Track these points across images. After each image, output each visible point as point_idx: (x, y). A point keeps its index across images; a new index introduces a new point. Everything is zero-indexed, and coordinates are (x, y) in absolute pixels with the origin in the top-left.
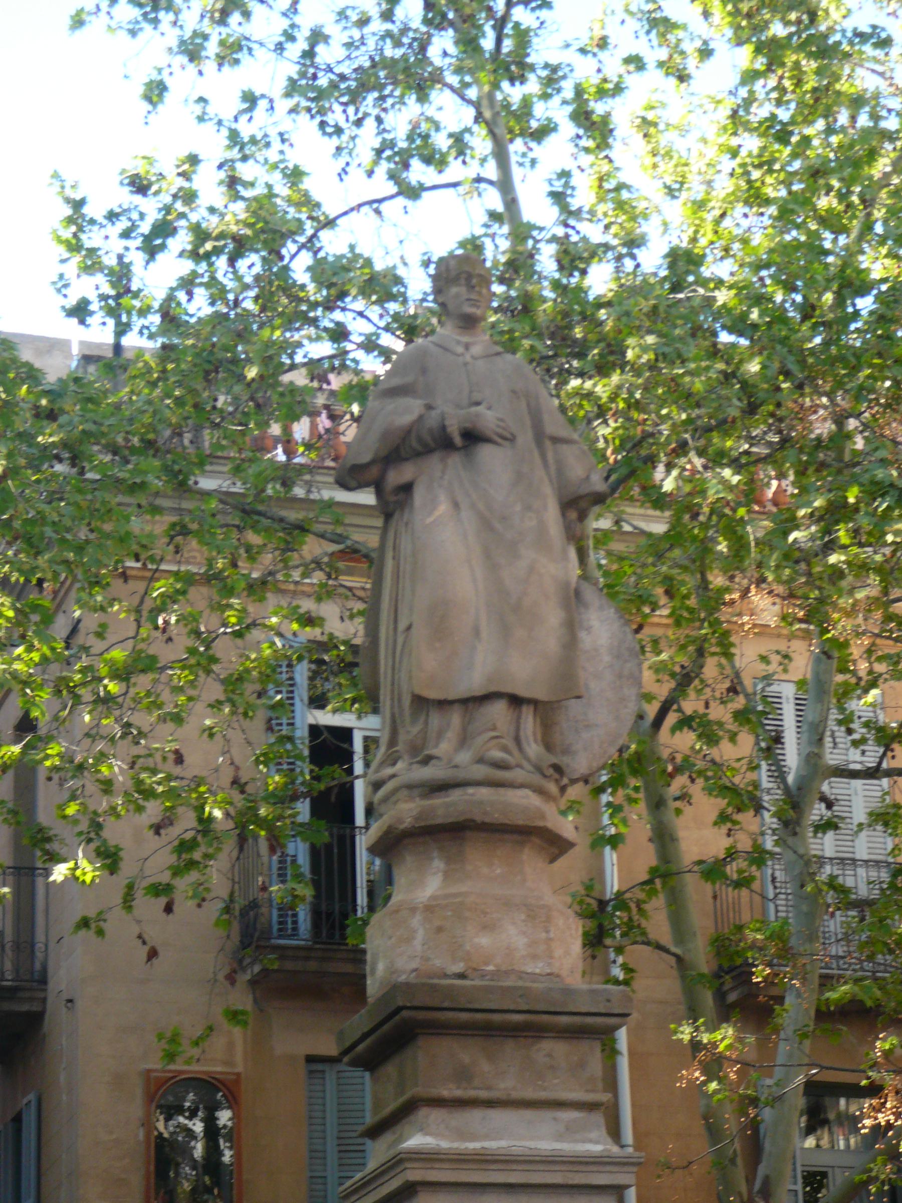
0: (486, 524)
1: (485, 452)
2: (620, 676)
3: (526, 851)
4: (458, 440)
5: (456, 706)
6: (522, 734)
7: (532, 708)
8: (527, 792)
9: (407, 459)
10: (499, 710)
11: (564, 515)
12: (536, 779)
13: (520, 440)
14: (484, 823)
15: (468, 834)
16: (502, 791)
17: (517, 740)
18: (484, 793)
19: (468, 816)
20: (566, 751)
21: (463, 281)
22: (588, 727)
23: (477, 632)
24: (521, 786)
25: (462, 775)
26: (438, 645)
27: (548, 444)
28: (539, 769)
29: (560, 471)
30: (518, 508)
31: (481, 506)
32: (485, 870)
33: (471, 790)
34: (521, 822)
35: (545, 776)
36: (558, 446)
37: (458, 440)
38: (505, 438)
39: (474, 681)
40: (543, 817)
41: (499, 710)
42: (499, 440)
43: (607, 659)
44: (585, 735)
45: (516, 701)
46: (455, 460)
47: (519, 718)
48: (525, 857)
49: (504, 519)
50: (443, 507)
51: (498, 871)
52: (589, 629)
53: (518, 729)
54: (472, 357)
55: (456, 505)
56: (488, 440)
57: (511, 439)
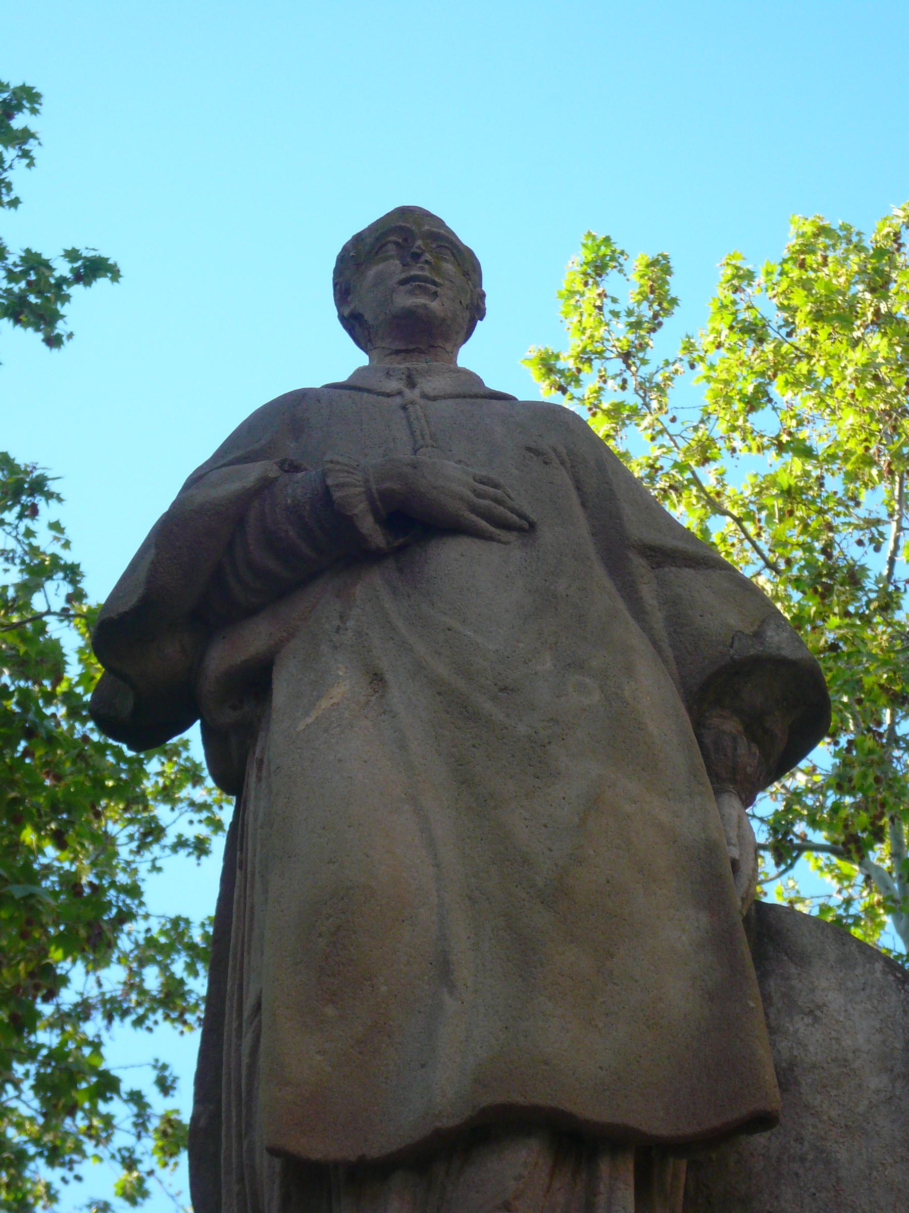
0: (457, 708)
1: (451, 557)
4: (377, 537)
7: (627, 1169)
9: (251, 612)
11: (699, 725)
13: (548, 535)
21: (391, 249)
23: (444, 969)
26: (330, 1011)
27: (638, 563)
29: (677, 622)
30: (547, 663)
31: (442, 669)
36: (670, 572)
37: (377, 537)
38: (506, 526)
43: (876, 1082)
47: (592, 1192)
49: (505, 690)
50: (343, 687)
52: (814, 1013)
54: (425, 396)
55: (377, 679)
56: (455, 528)
57: (526, 529)
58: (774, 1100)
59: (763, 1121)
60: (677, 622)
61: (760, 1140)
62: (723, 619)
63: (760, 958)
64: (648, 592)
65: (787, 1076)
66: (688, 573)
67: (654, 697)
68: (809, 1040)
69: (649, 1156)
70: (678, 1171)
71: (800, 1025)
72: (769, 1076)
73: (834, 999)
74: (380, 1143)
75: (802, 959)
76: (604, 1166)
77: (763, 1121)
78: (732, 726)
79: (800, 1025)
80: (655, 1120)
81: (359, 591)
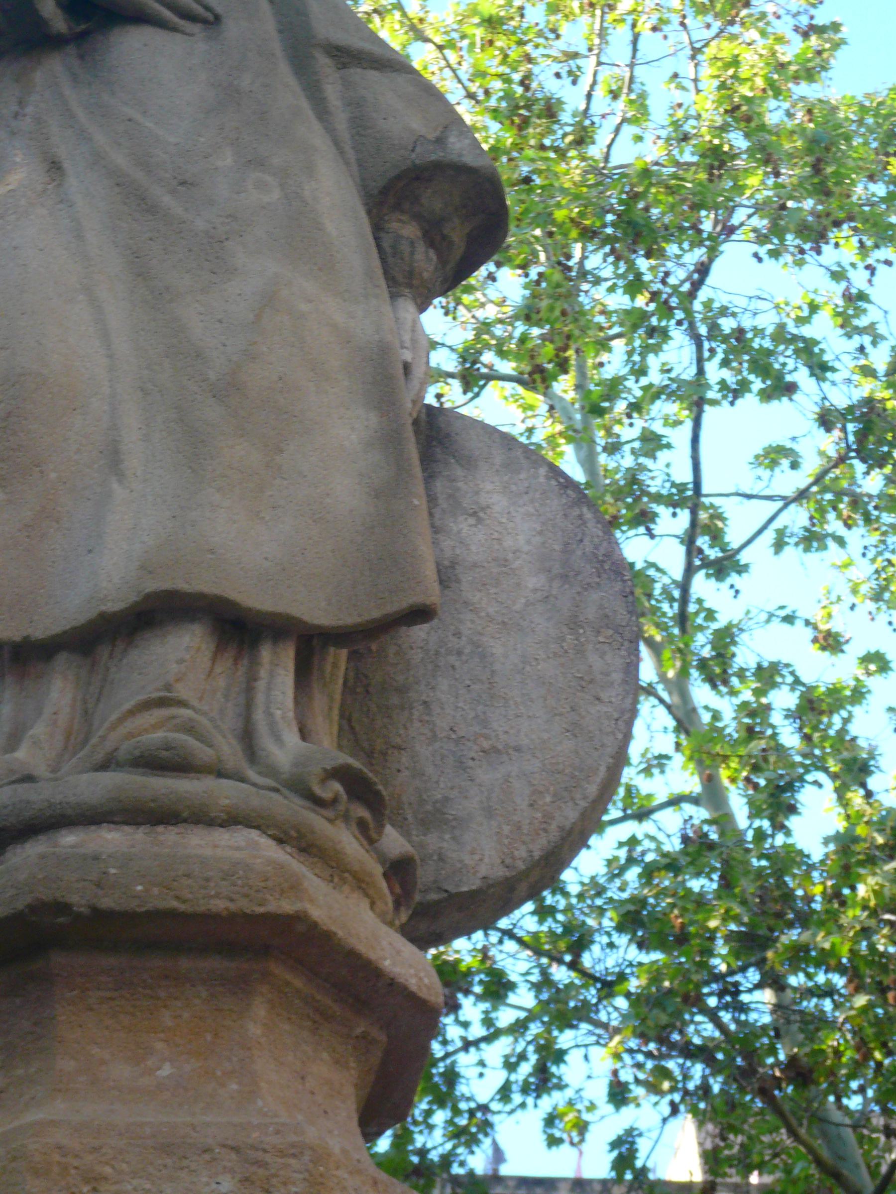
0: (134, 199)
2: (574, 623)
3: (260, 1009)
4: (59, 23)
5: (62, 659)
6: (259, 716)
7: (288, 655)
8: (254, 834)
10: (181, 654)
11: (378, 228)
12: (289, 807)
13: (232, 29)
14: (99, 915)
15: (58, 959)
16: (169, 835)
17: (247, 737)
18: (111, 839)
19: (45, 894)
20: (435, 818)
22: (492, 753)
23: (114, 459)
24: (233, 820)
25: (39, 796)
27: (323, 62)
28: (300, 788)
29: (360, 123)
30: (227, 159)
31: (120, 159)
32: (121, 1071)
33: (69, 839)
34: (219, 905)
35: (318, 802)
36: (355, 73)
39: (107, 572)
40: (294, 887)
41: (181, 654)
42: (175, 19)
43: (533, 582)
44: (485, 775)
45: (238, 629)
46: (54, 68)
47: (252, 678)
48: (255, 1030)
51: (166, 1070)
52: (477, 514)
53: (249, 706)
55: (55, 167)
58: (432, 594)
59: (421, 614)
60: (360, 123)
61: (420, 632)
62: (405, 124)
63: (427, 459)
64: (332, 92)
65: (447, 576)
66: (373, 75)
67: (335, 201)
68: (470, 539)
69: (310, 645)
70: (337, 660)
71: (463, 526)
72: (430, 572)
73: (498, 502)
74: (45, 624)
75: (468, 462)
76: (266, 653)
77: (421, 614)
78: (410, 230)
79: (463, 526)
80: (318, 611)
81: (38, 76)
